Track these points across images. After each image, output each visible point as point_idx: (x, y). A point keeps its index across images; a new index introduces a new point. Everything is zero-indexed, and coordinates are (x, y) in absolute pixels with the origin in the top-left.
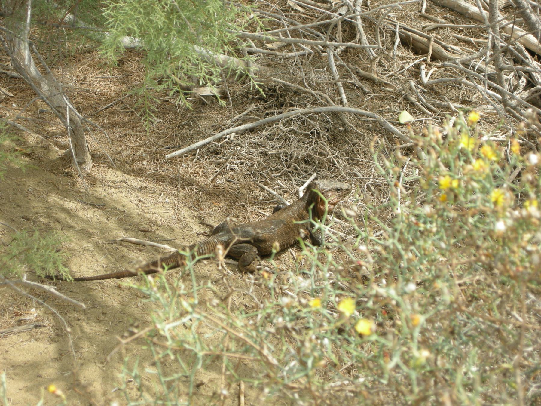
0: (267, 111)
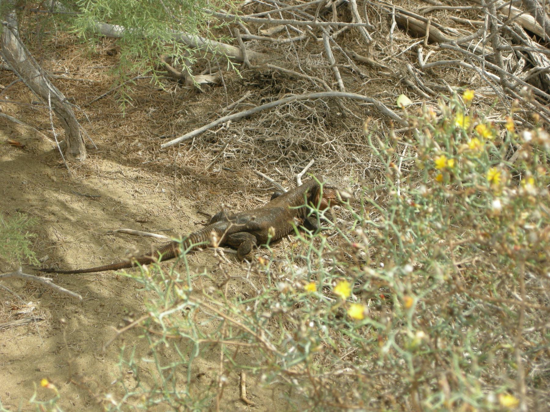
0: (263, 98)
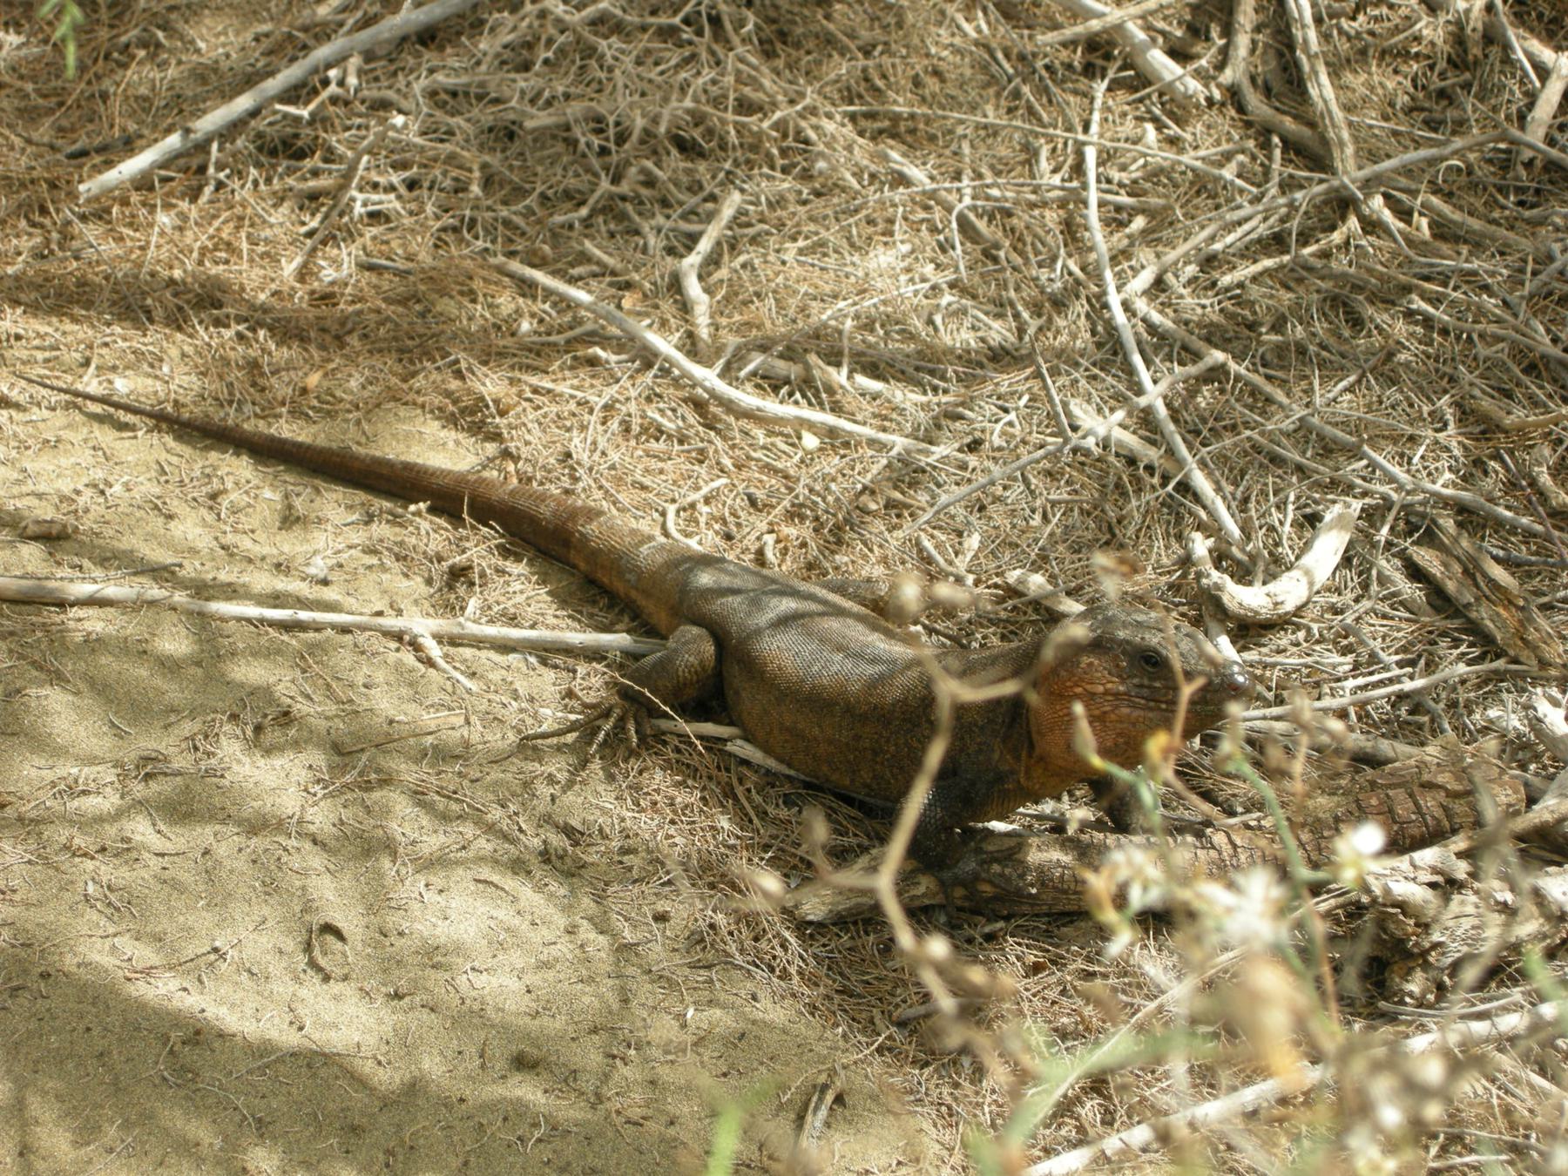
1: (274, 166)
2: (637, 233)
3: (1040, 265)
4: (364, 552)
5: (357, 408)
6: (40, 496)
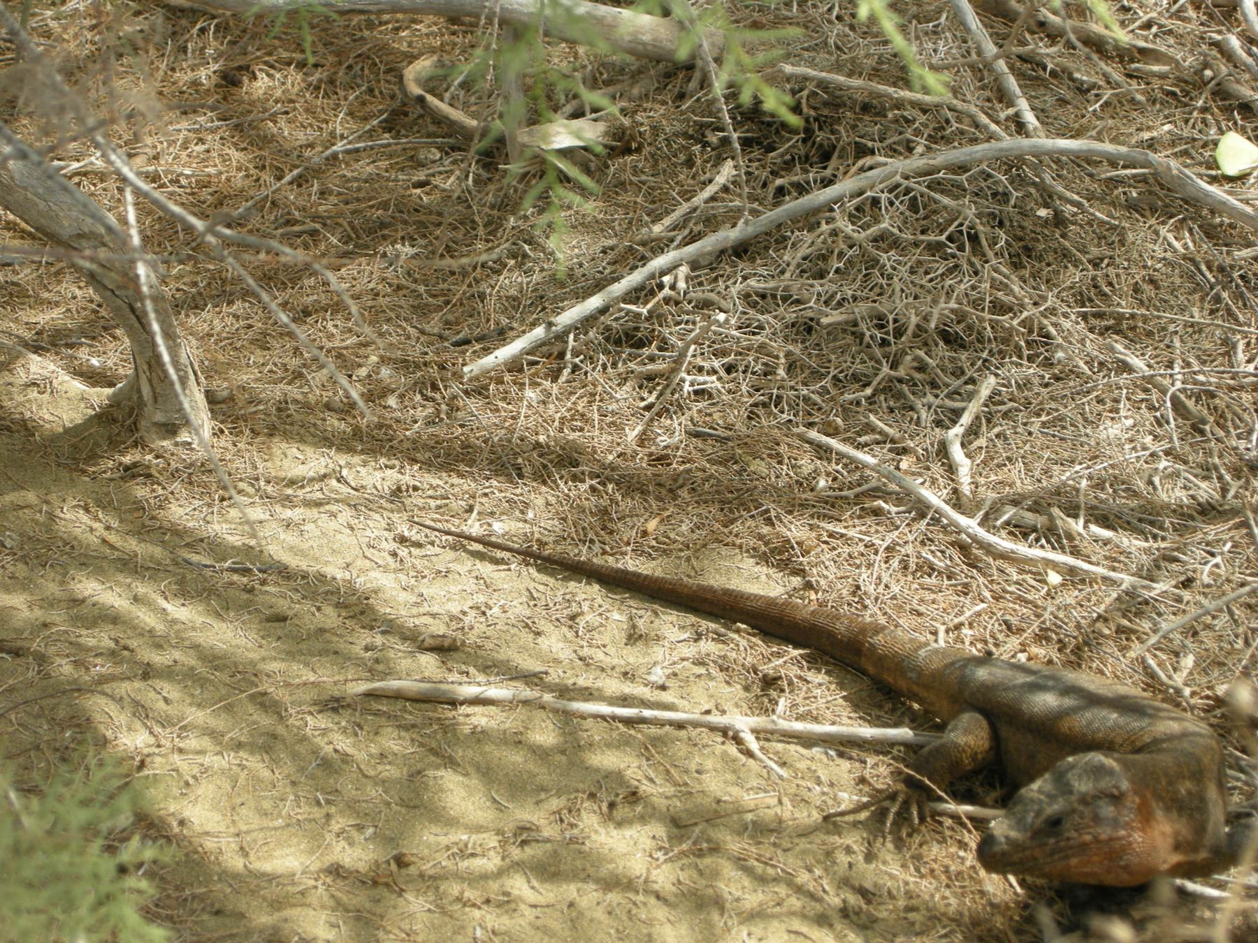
0: (779, 182)
1: (618, 353)
2: (912, 409)
3: (1239, 438)
4: (693, 663)
5: (688, 547)
6: (434, 616)
